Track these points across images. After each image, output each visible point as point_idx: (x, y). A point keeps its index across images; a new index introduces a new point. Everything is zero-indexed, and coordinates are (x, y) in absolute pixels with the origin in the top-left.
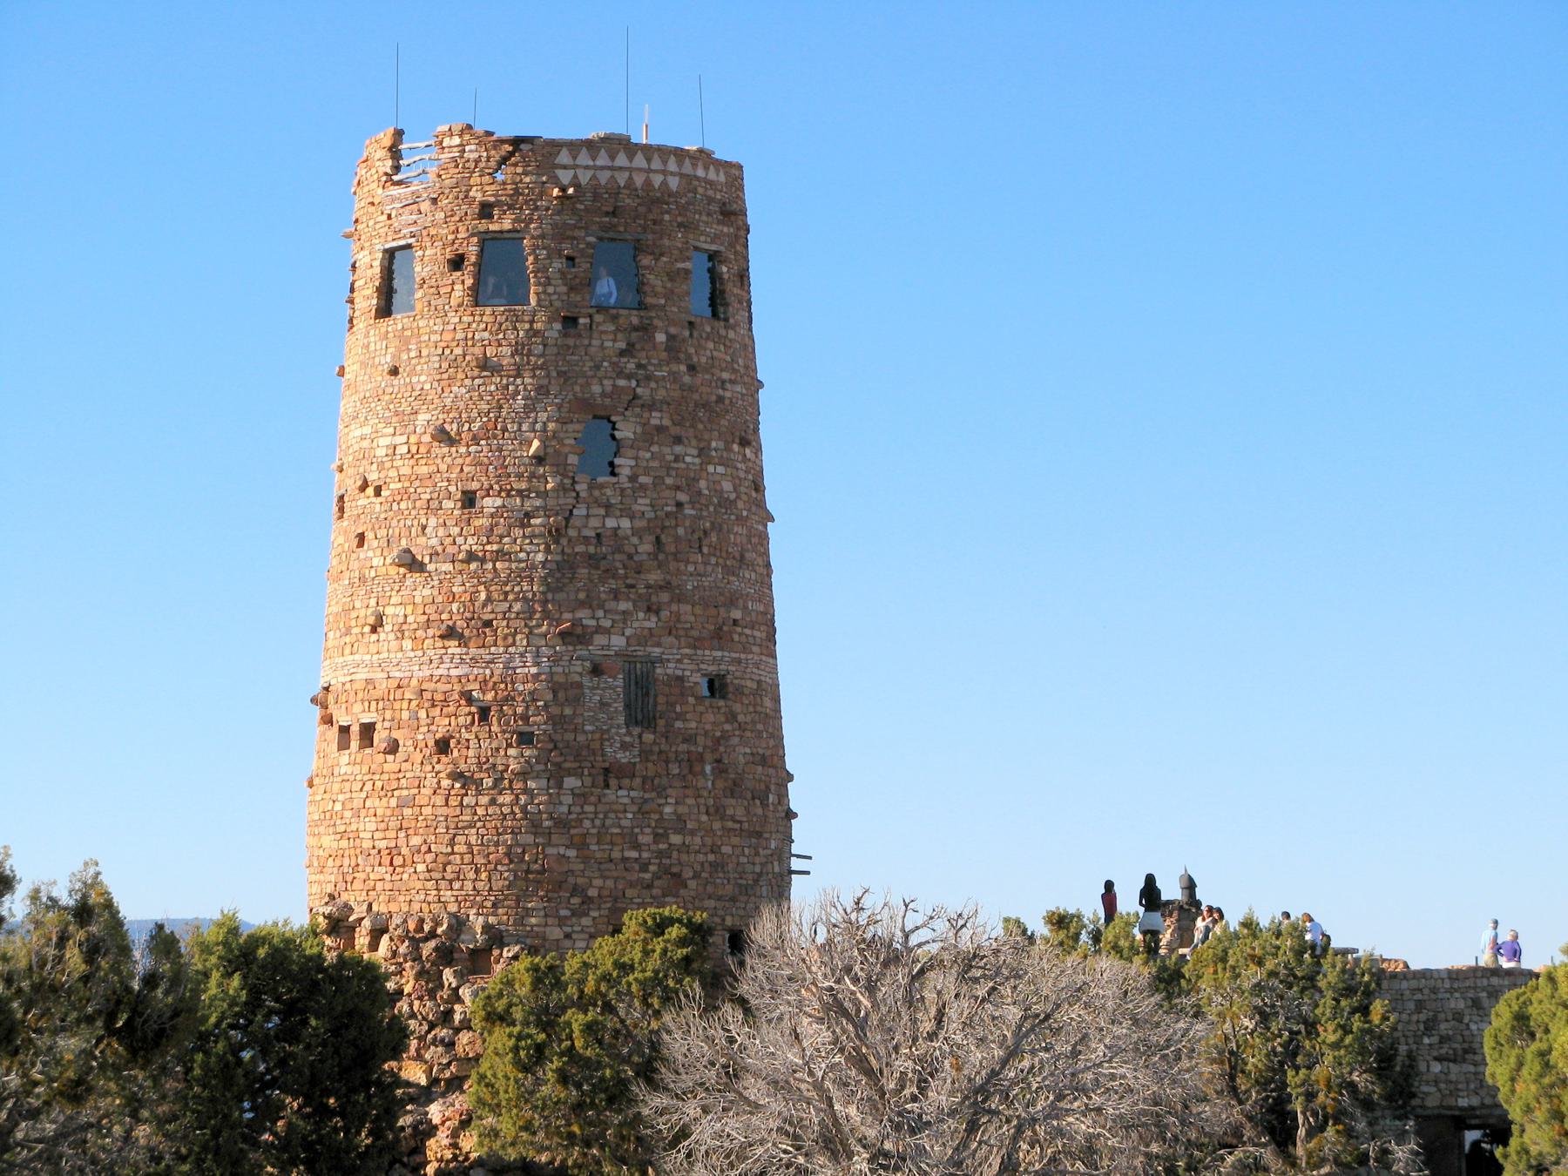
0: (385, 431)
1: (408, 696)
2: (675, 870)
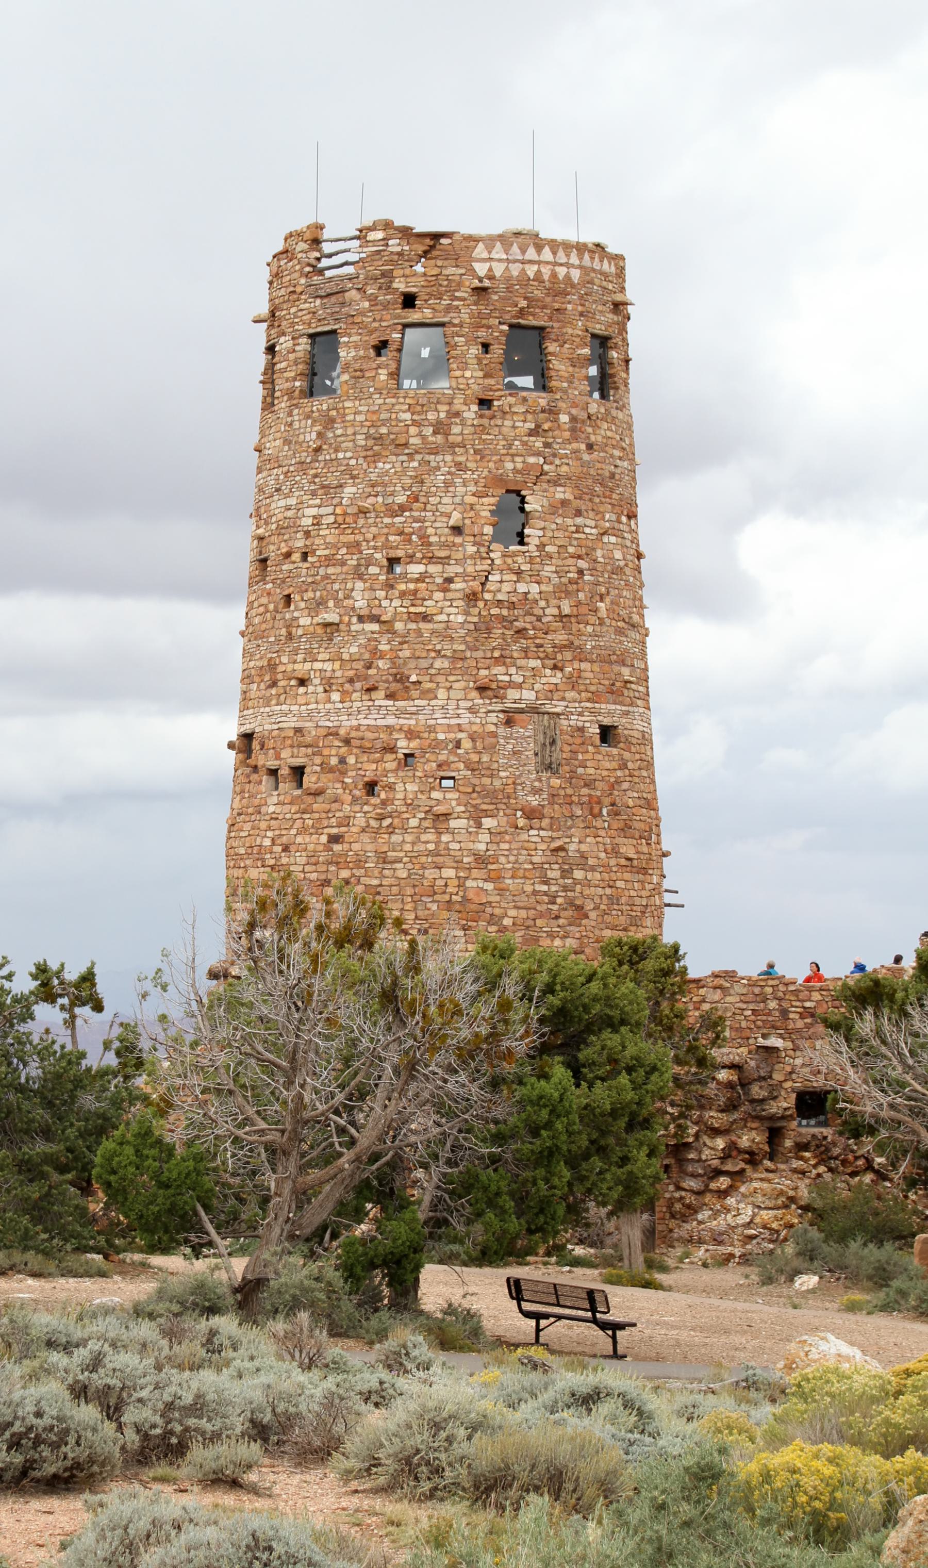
0: (311, 502)
2: (578, 902)
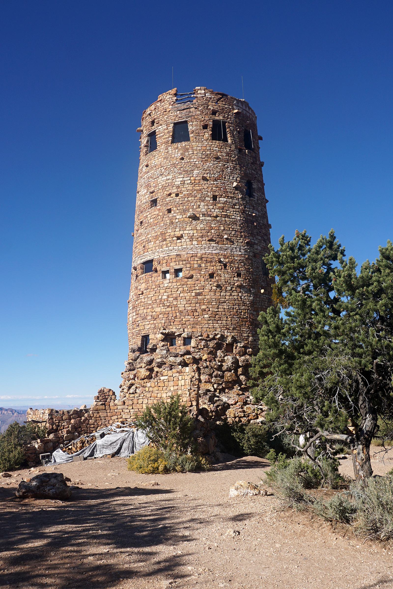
0: (179, 176)
1: (196, 259)
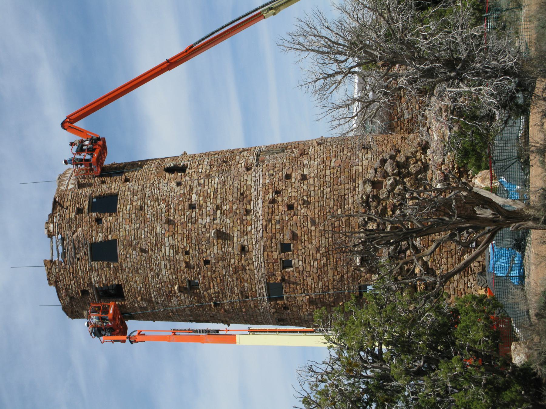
0: (163, 251)
